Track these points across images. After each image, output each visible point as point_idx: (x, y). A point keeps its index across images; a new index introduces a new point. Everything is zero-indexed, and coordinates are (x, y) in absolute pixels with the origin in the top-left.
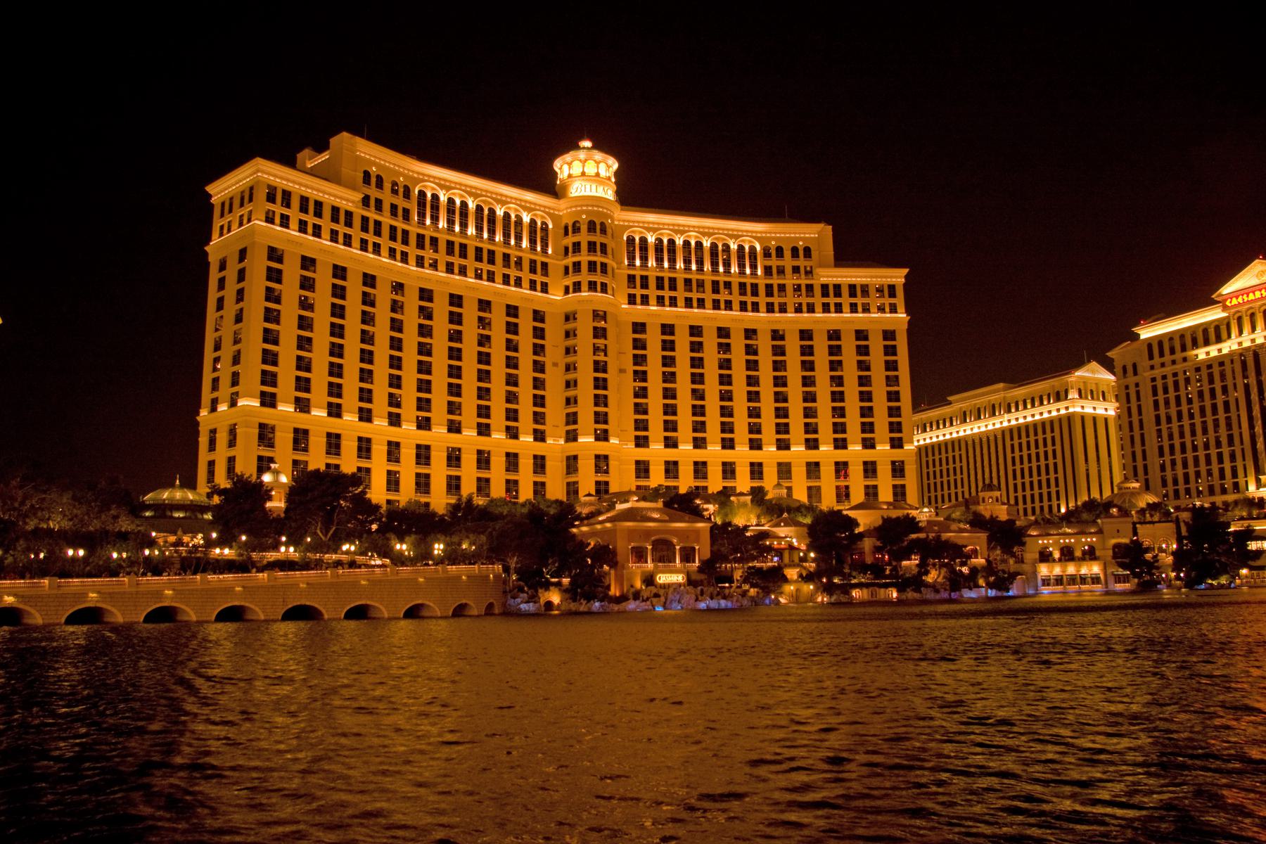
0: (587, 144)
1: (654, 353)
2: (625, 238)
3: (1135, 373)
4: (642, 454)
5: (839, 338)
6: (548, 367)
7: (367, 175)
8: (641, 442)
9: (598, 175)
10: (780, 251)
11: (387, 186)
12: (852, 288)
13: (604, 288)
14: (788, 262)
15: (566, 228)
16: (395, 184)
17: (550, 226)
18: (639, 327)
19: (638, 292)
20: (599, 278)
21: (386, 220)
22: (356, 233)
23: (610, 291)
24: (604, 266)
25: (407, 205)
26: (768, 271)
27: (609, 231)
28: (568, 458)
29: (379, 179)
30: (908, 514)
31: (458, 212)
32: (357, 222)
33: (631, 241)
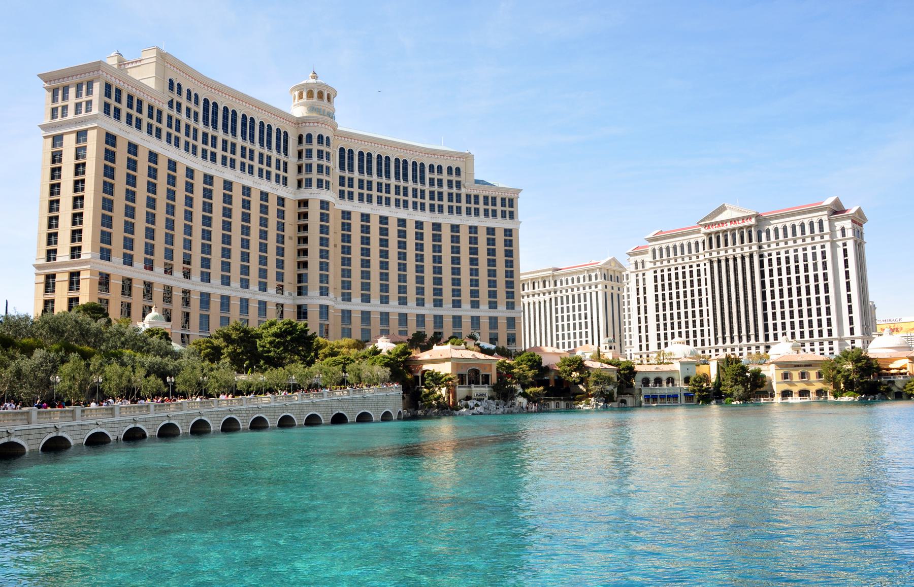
1: (356, 234)
3: (643, 267)
4: (346, 306)
6: (286, 239)
7: (171, 82)
8: (347, 297)
10: (440, 168)
12: (486, 198)
14: (445, 177)
15: (300, 138)
16: (189, 92)
18: (346, 215)
19: (346, 189)
20: (324, 177)
21: (183, 117)
23: (331, 188)
24: (328, 168)
25: (197, 110)
26: (432, 181)
28: (299, 307)
33: (342, 150)
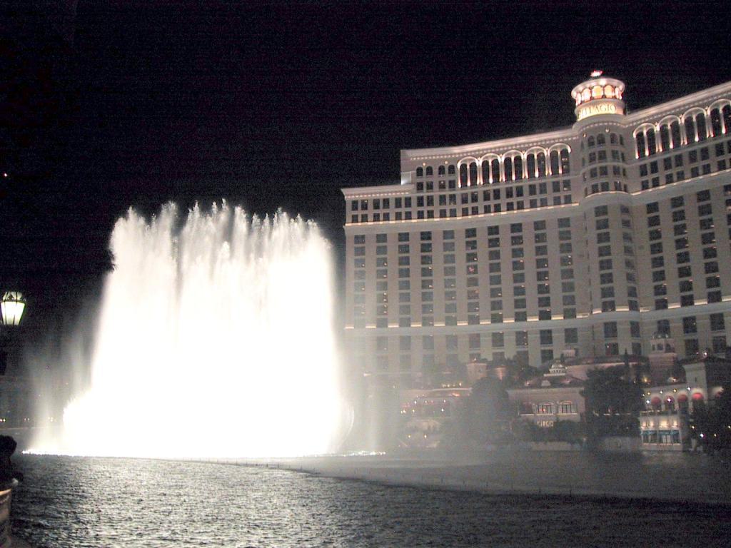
0: (596, 74)
2: (634, 135)
5: (429, 238)
9: (592, 98)
11: (435, 171)
13: (605, 187)
17: (569, 150)
18: (652, 207)
21: (436, 193)
22: (414, 209)
27: (608, 139)
29: (430, 170)
30: (603, 367)
31: (491, 169)
32: (414, 202)
33: (640, 135)
